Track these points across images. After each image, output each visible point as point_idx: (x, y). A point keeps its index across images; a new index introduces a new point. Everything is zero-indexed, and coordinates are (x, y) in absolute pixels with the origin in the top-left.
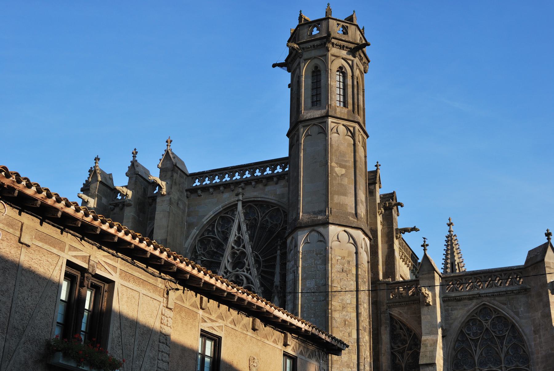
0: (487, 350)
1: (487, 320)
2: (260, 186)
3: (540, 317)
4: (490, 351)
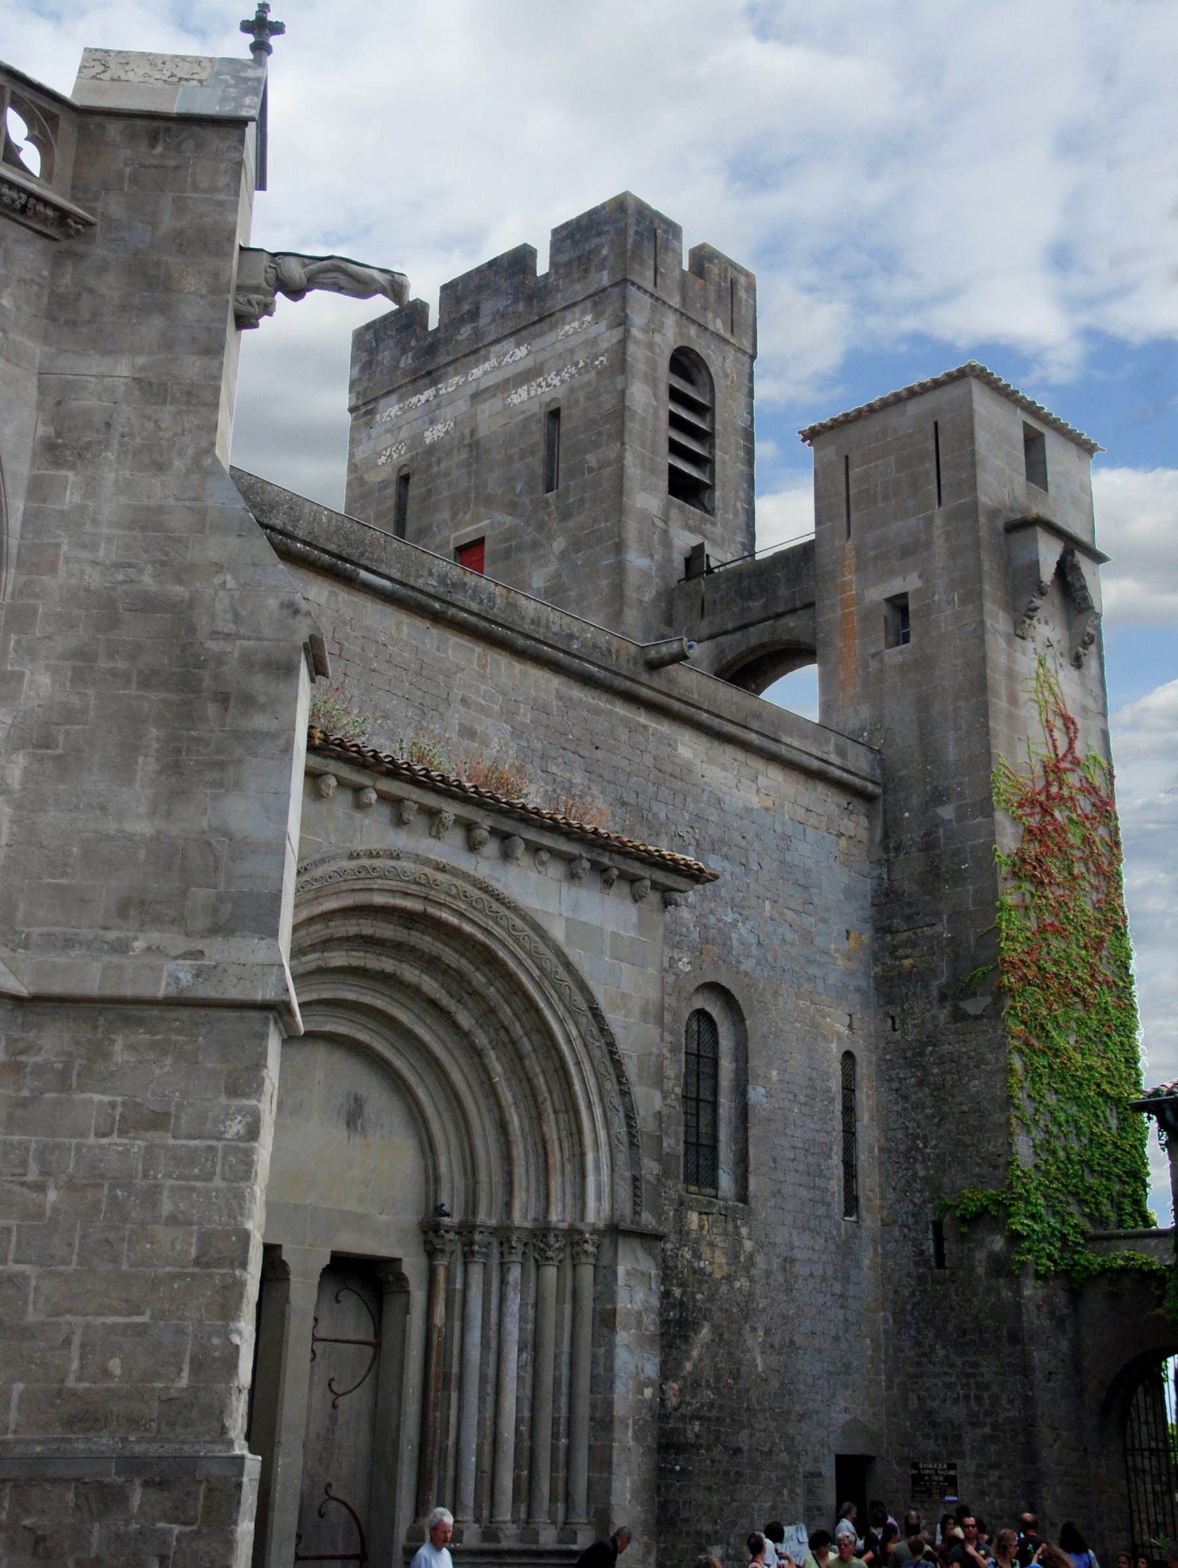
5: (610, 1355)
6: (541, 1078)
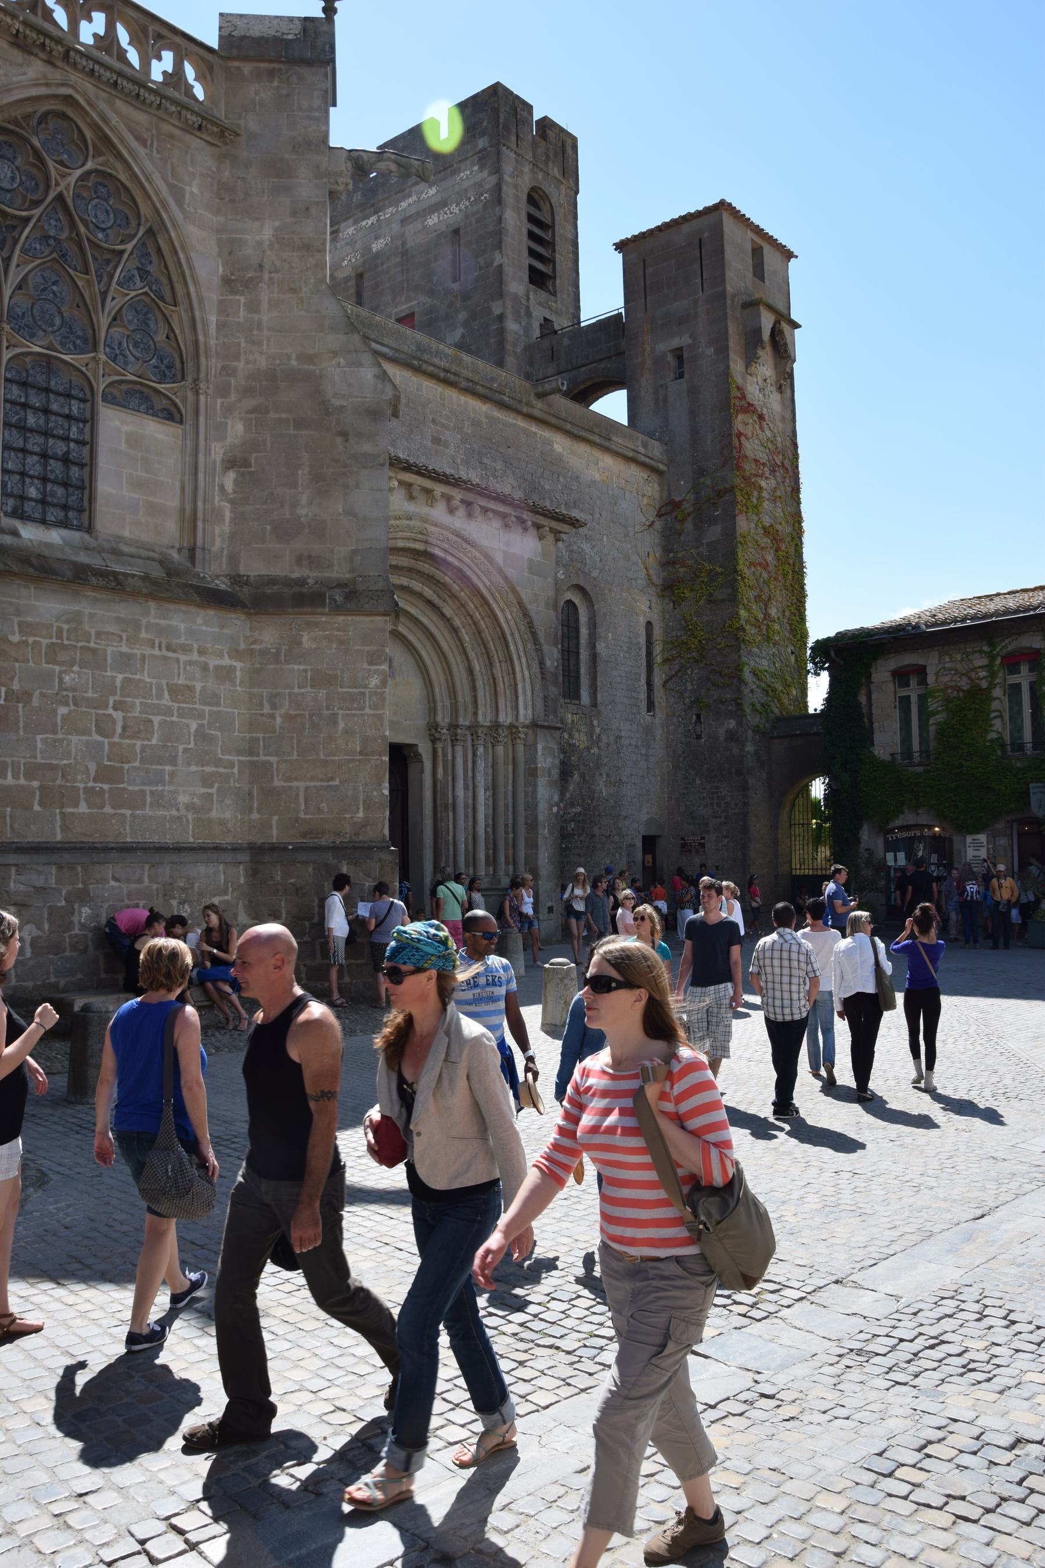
0: (44, 278)
3: (267, 243)
4: (55, 288)
5: (535, 792)
6: (491, 643)
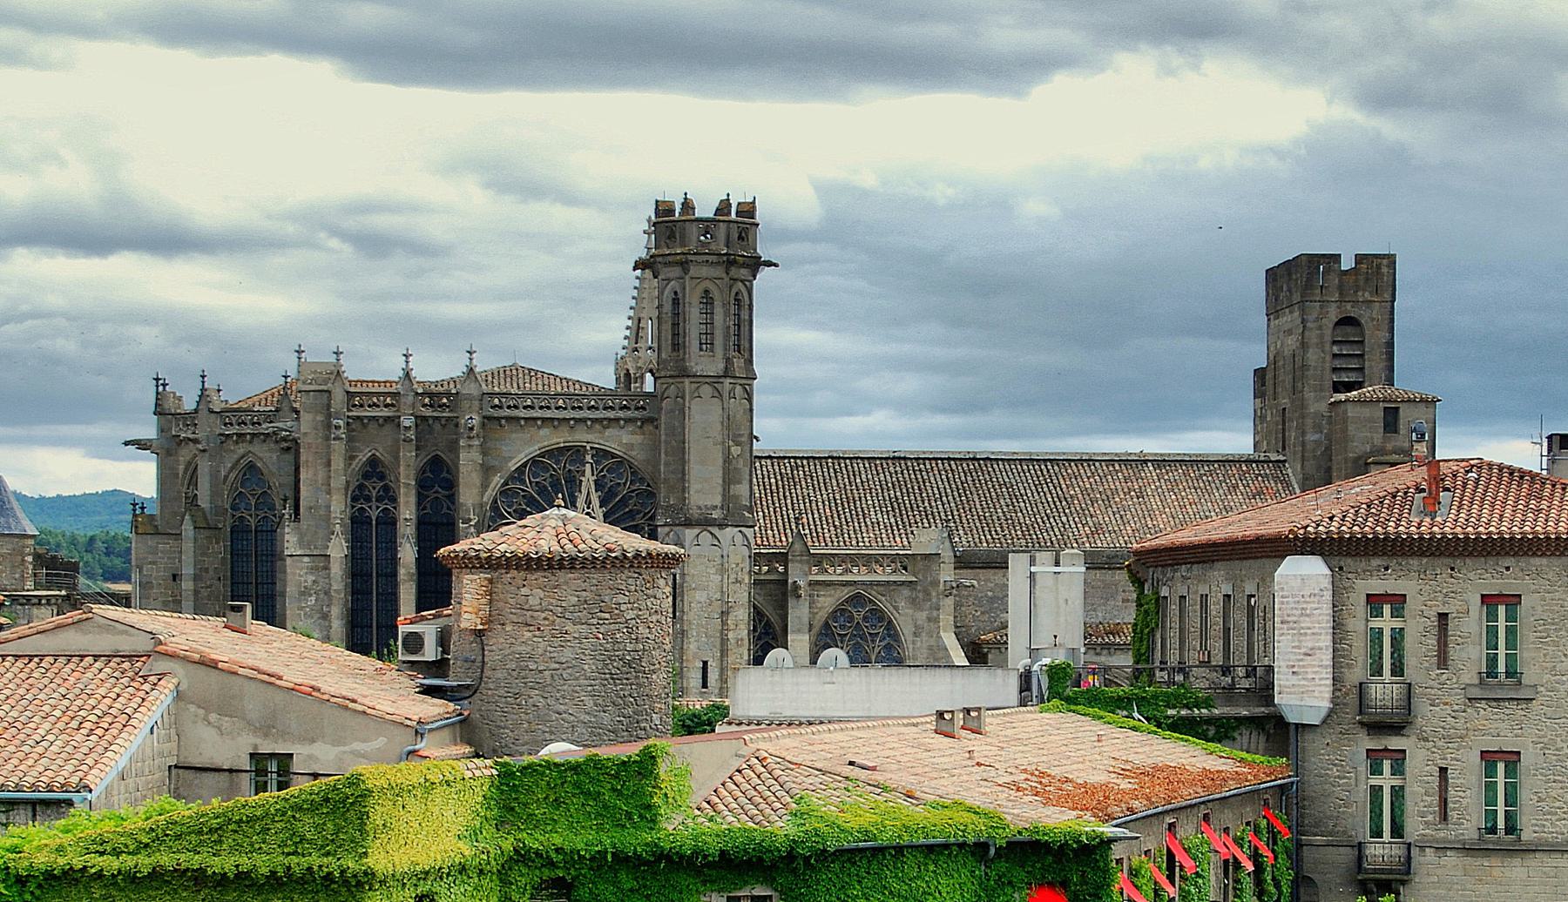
1: (859, 611)
2: (597, 426)
